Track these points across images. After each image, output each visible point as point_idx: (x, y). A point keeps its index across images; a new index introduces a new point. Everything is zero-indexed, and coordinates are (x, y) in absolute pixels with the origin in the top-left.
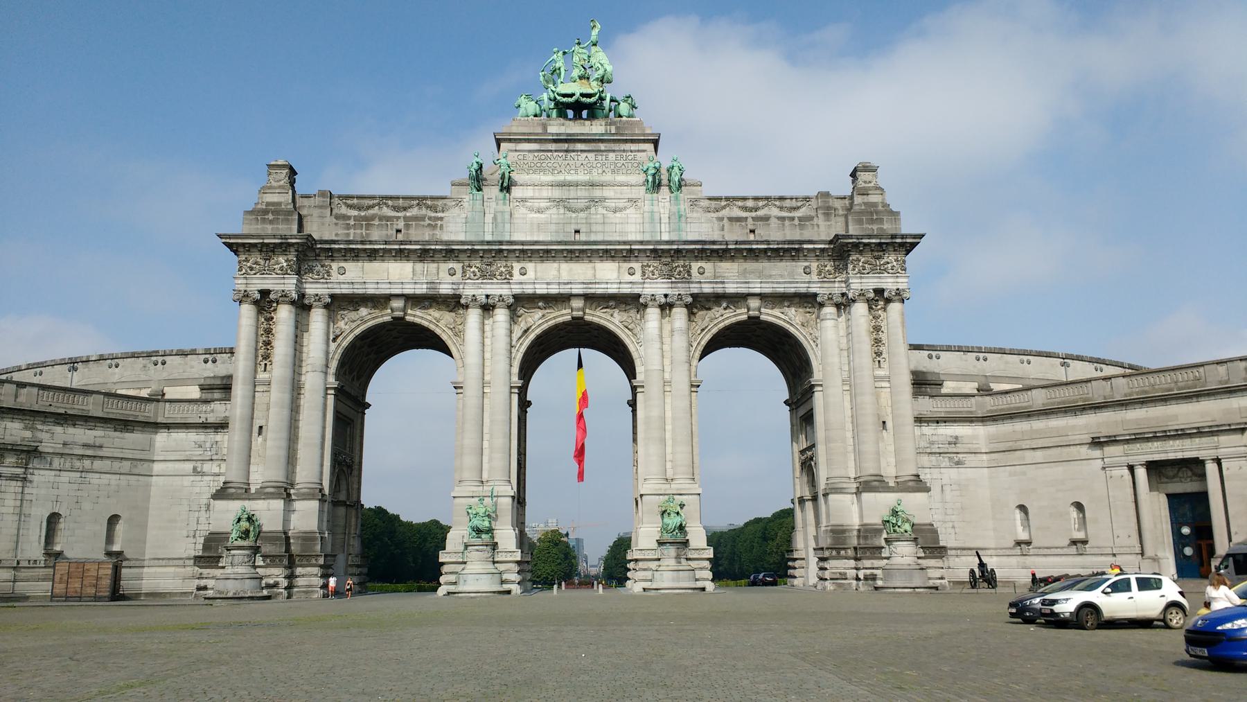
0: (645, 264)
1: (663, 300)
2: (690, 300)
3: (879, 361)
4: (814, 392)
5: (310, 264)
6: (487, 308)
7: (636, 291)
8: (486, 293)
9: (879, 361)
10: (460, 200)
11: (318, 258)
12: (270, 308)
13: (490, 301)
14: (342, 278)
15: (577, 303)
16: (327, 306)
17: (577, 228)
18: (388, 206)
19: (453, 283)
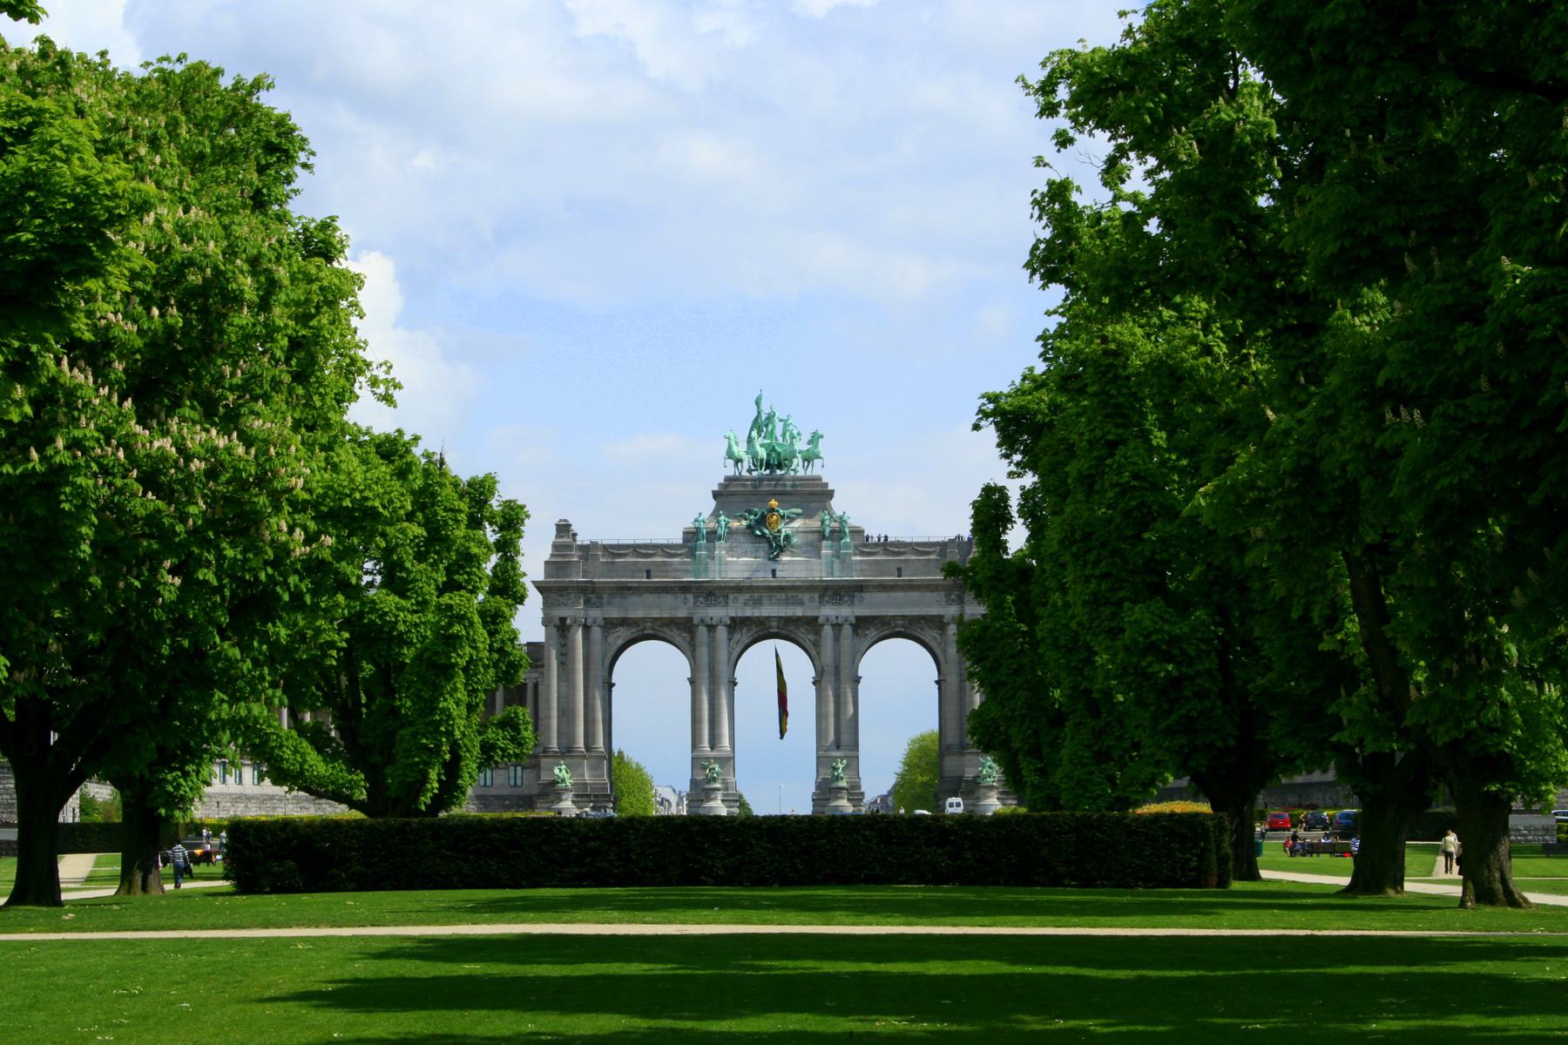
1: (835, 622)
6: (711, 628)
7: (815, 614)
13: (714, 623)
15: (775, 624)
16: (600, 626)
17: (774, 567)
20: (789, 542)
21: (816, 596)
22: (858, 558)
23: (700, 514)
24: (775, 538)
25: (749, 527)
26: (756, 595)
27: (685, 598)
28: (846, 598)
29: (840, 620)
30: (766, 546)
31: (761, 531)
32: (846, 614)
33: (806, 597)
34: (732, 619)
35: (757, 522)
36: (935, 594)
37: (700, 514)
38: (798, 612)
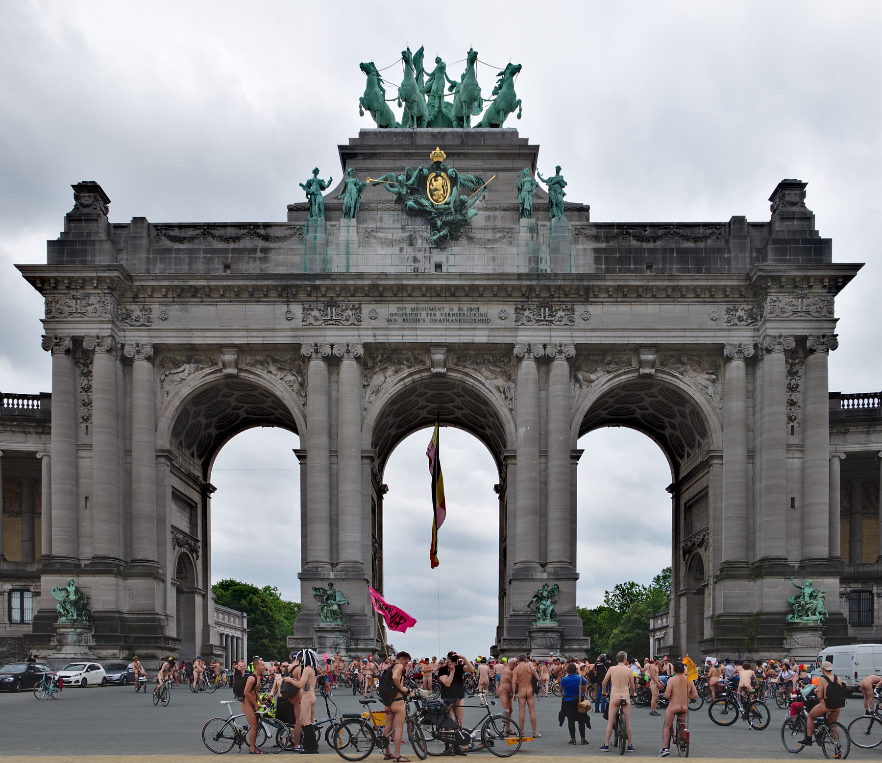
0: (520, 306)
1: (541, 352)
2: (572, 352)
3: (793, 427)
4: (711, 465)
5: (128, 307)
6: (333, 362)
8: (331, 342)
9: (793, 427)
10: (298, 227)
11: (136, 300)
12: (87, 359)
13: (336, 352)
14: (164, 325)
16: (148, 359)
18: (214, 236)
19: (292, 330)
20: (464, 215)
21: (510, 310)
22: (581, 247)
23: (316, 172)
24: (441, 213)
25: (400, 199)
26: (409, 307)
27: (289, 312)
28: (561, 313)
29: (550, 351)
30: (421, 228)
31: (416, 202)
32: (556, 341)
33: (493, 310)
34: (366, 346)
35: (413, 191)
36: (710, 308)
37: (316, 172)
38: (481, 337)
